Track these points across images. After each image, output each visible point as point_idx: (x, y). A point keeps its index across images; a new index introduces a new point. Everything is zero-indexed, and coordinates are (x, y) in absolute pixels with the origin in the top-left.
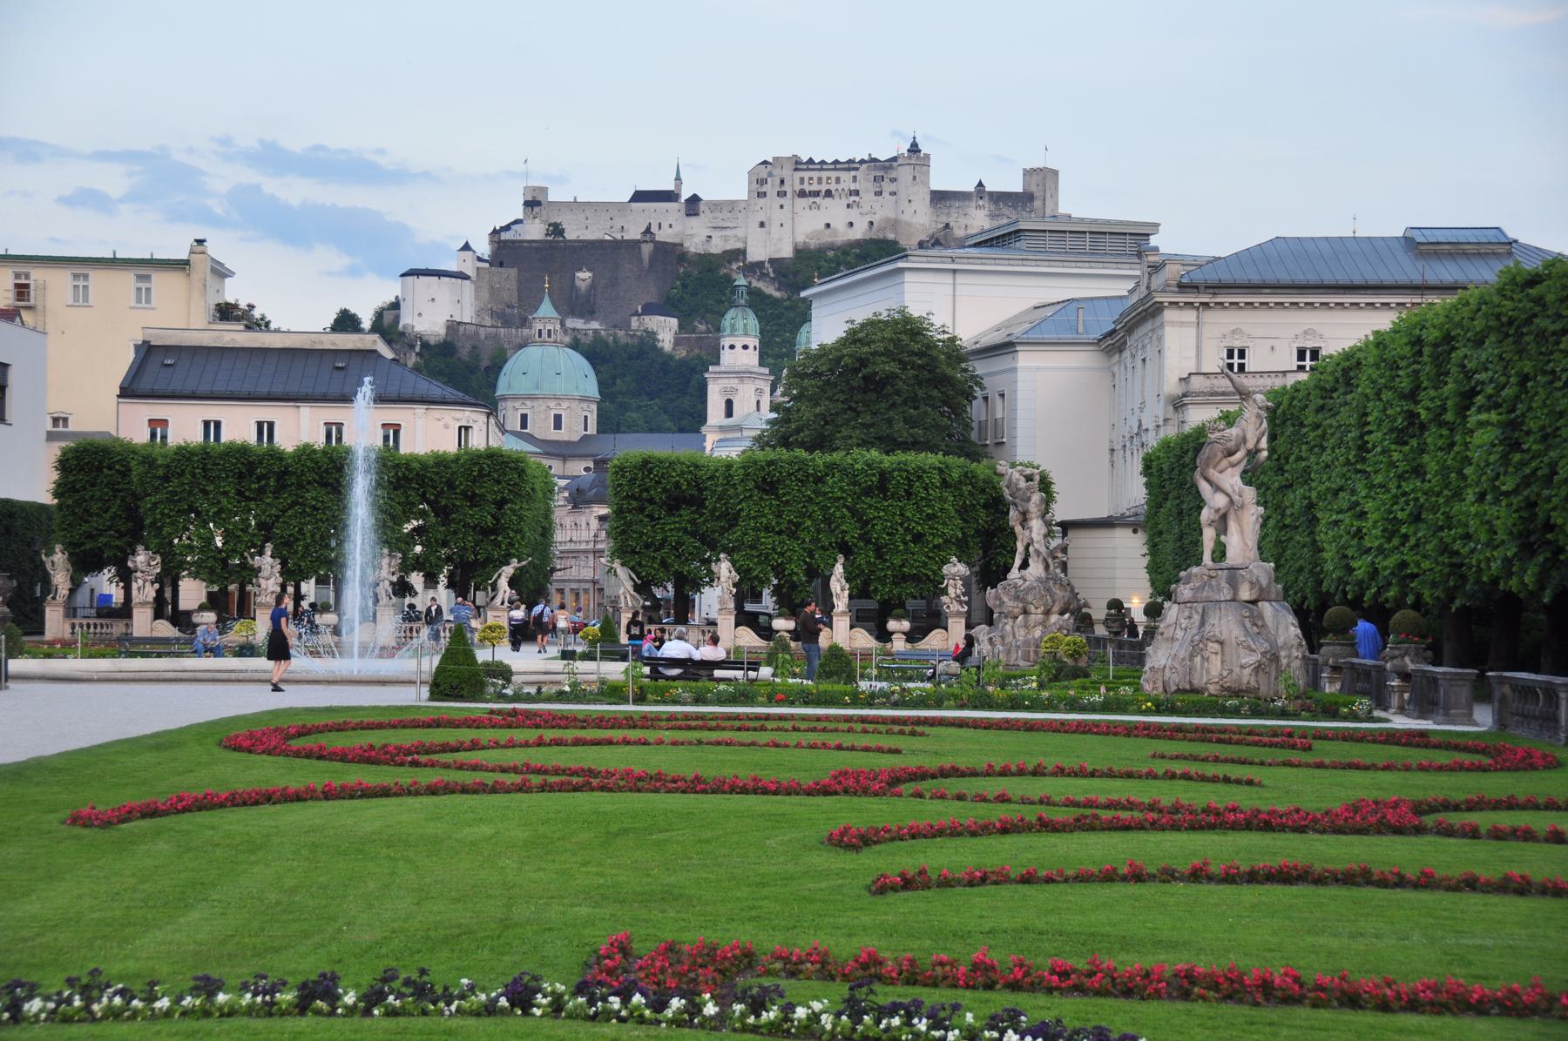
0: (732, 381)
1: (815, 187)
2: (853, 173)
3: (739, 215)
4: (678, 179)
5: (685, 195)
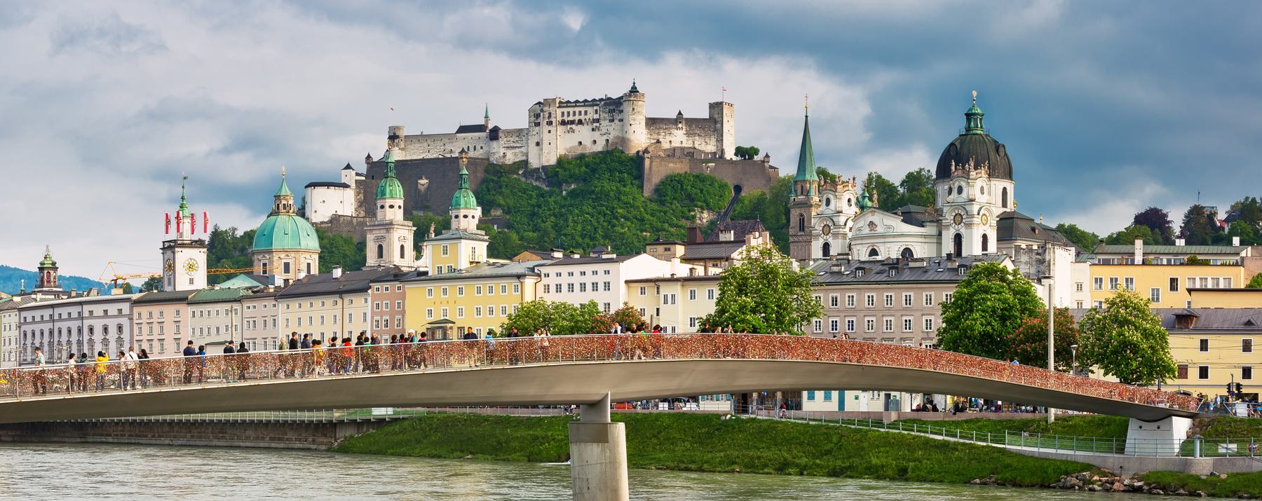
1: (571, 118)
2: (595, 108)
4: (486, 117)
5: (490, 126)
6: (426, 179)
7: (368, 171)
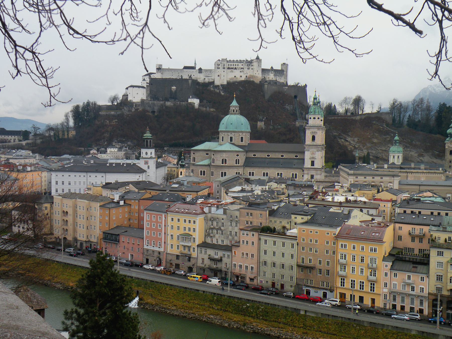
0: (315, 129)
1: (232, 67)
2: (242, 63)
4: (195, 64)
5: (197, 68)
6: (175, 86)
7: (150, 82)
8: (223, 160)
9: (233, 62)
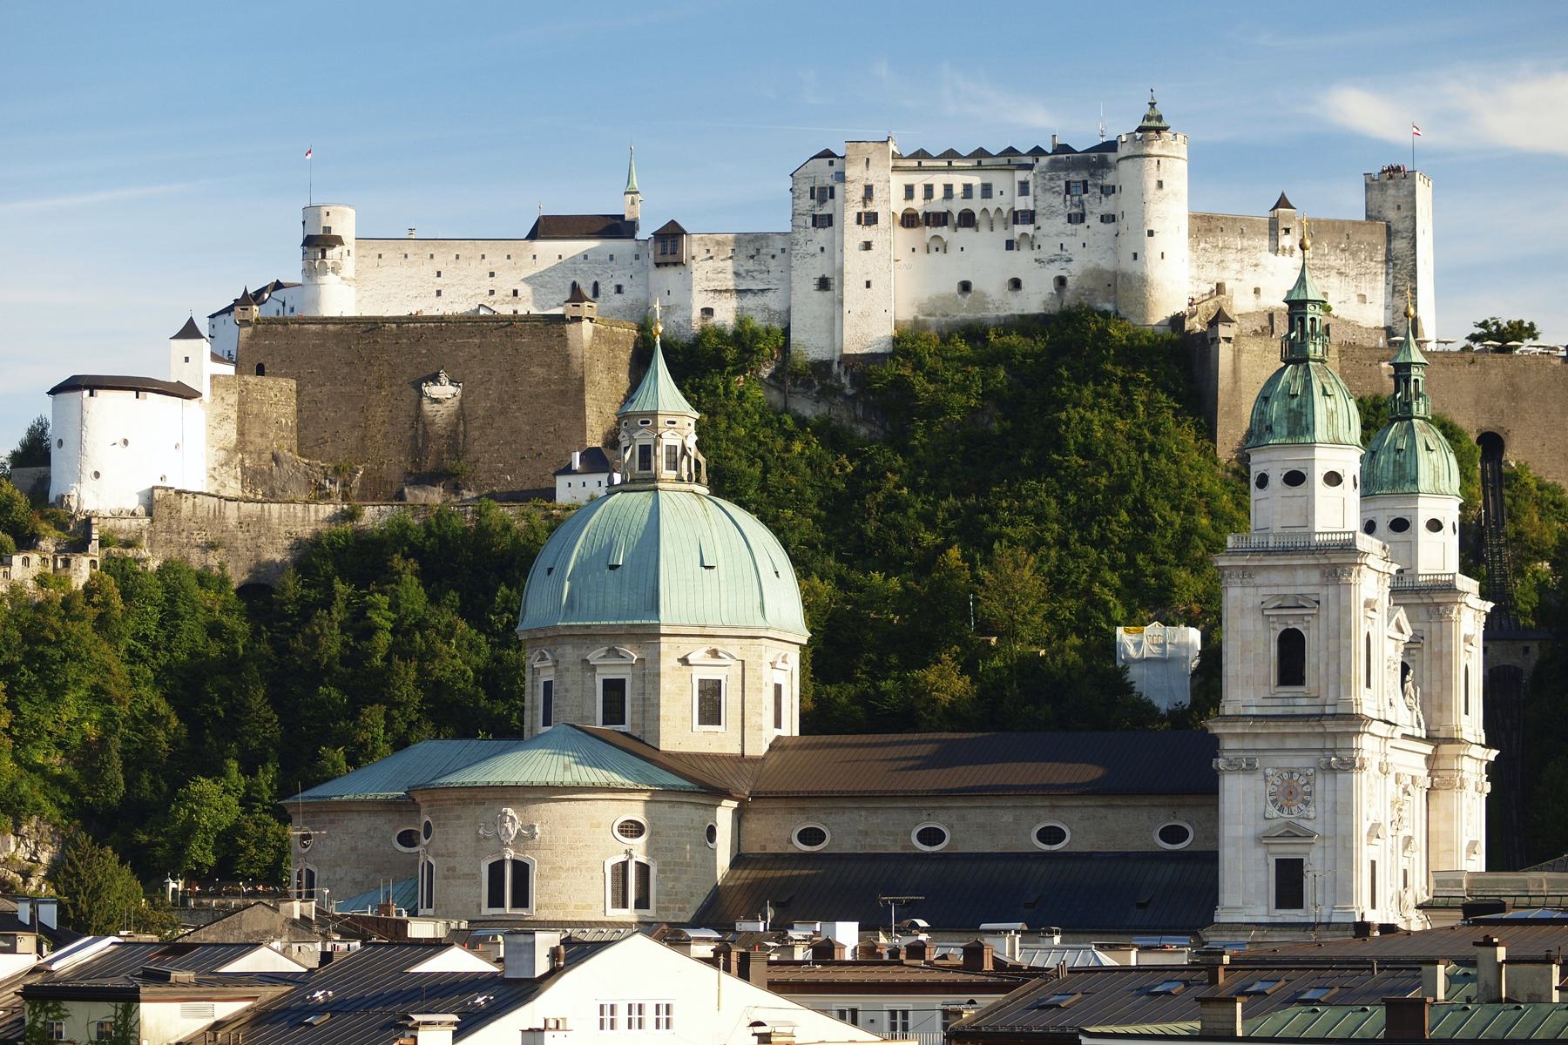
0: (1300, 576)
1: (938, 204)
2: (1021, 175)
3: (772, 264)
8: (496, 870)
9: (950, 169)
